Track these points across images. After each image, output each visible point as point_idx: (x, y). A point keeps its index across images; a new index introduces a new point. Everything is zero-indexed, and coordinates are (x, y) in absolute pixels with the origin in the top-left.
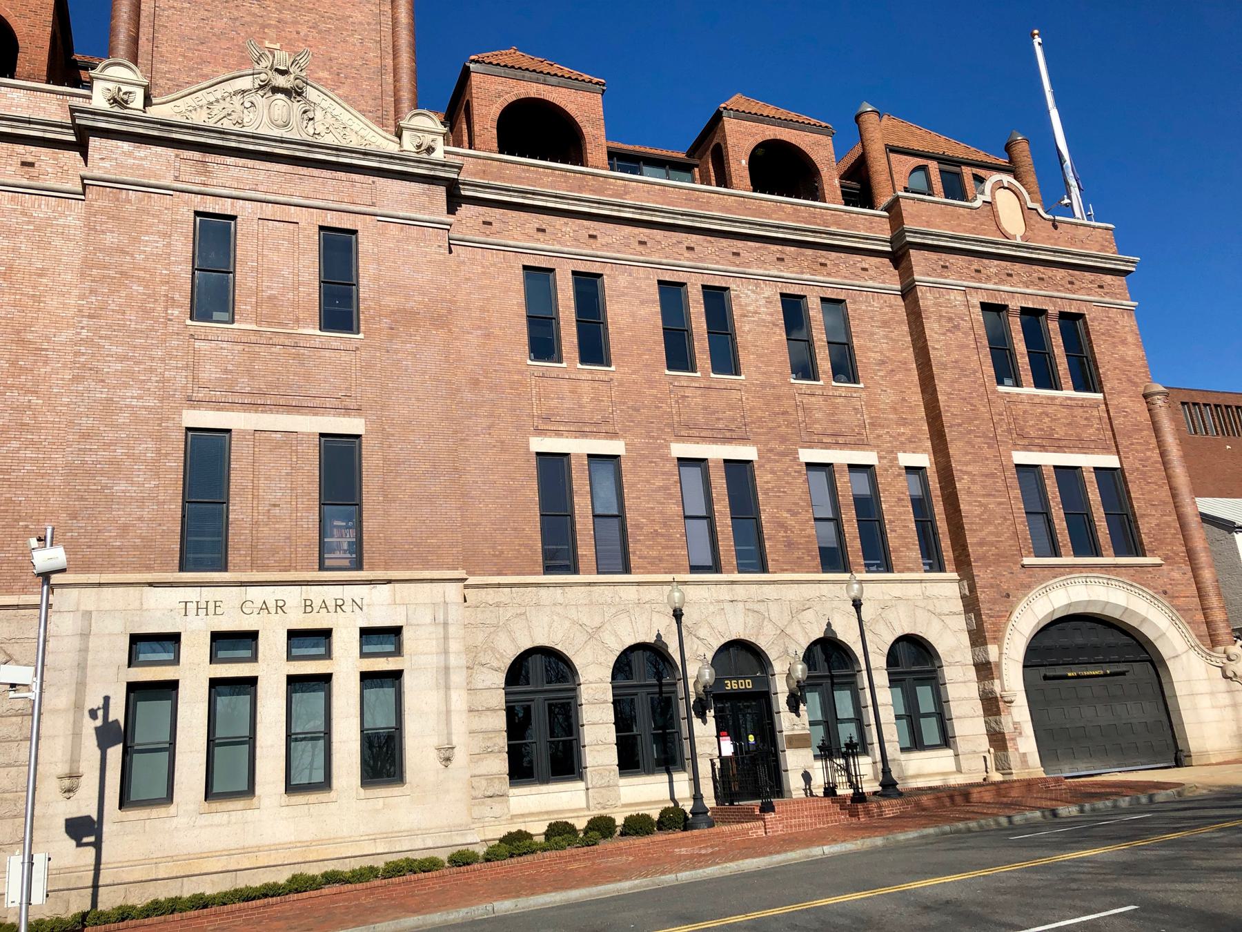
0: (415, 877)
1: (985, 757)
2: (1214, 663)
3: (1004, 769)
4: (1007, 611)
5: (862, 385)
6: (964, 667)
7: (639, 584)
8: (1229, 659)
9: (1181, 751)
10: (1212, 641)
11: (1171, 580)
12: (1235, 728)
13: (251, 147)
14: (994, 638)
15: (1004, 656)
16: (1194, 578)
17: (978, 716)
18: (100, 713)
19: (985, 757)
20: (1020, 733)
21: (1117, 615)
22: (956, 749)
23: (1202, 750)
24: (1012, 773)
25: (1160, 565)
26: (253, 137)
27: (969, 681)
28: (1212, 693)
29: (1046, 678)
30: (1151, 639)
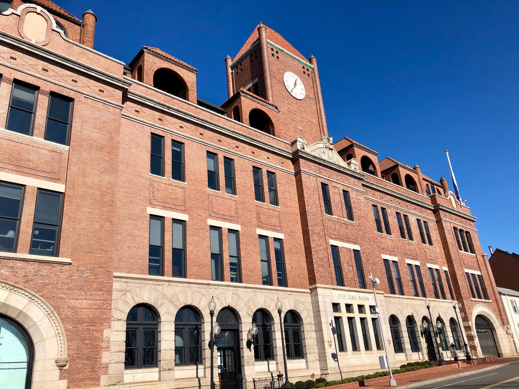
0: (409, 372)
5: (434, 247)
7: (407, 298)
8: (508, 329)
10: (503, 324)
13: (329, 165)
18: (331, 324)
25: (492, 303)
26: (330, 163)
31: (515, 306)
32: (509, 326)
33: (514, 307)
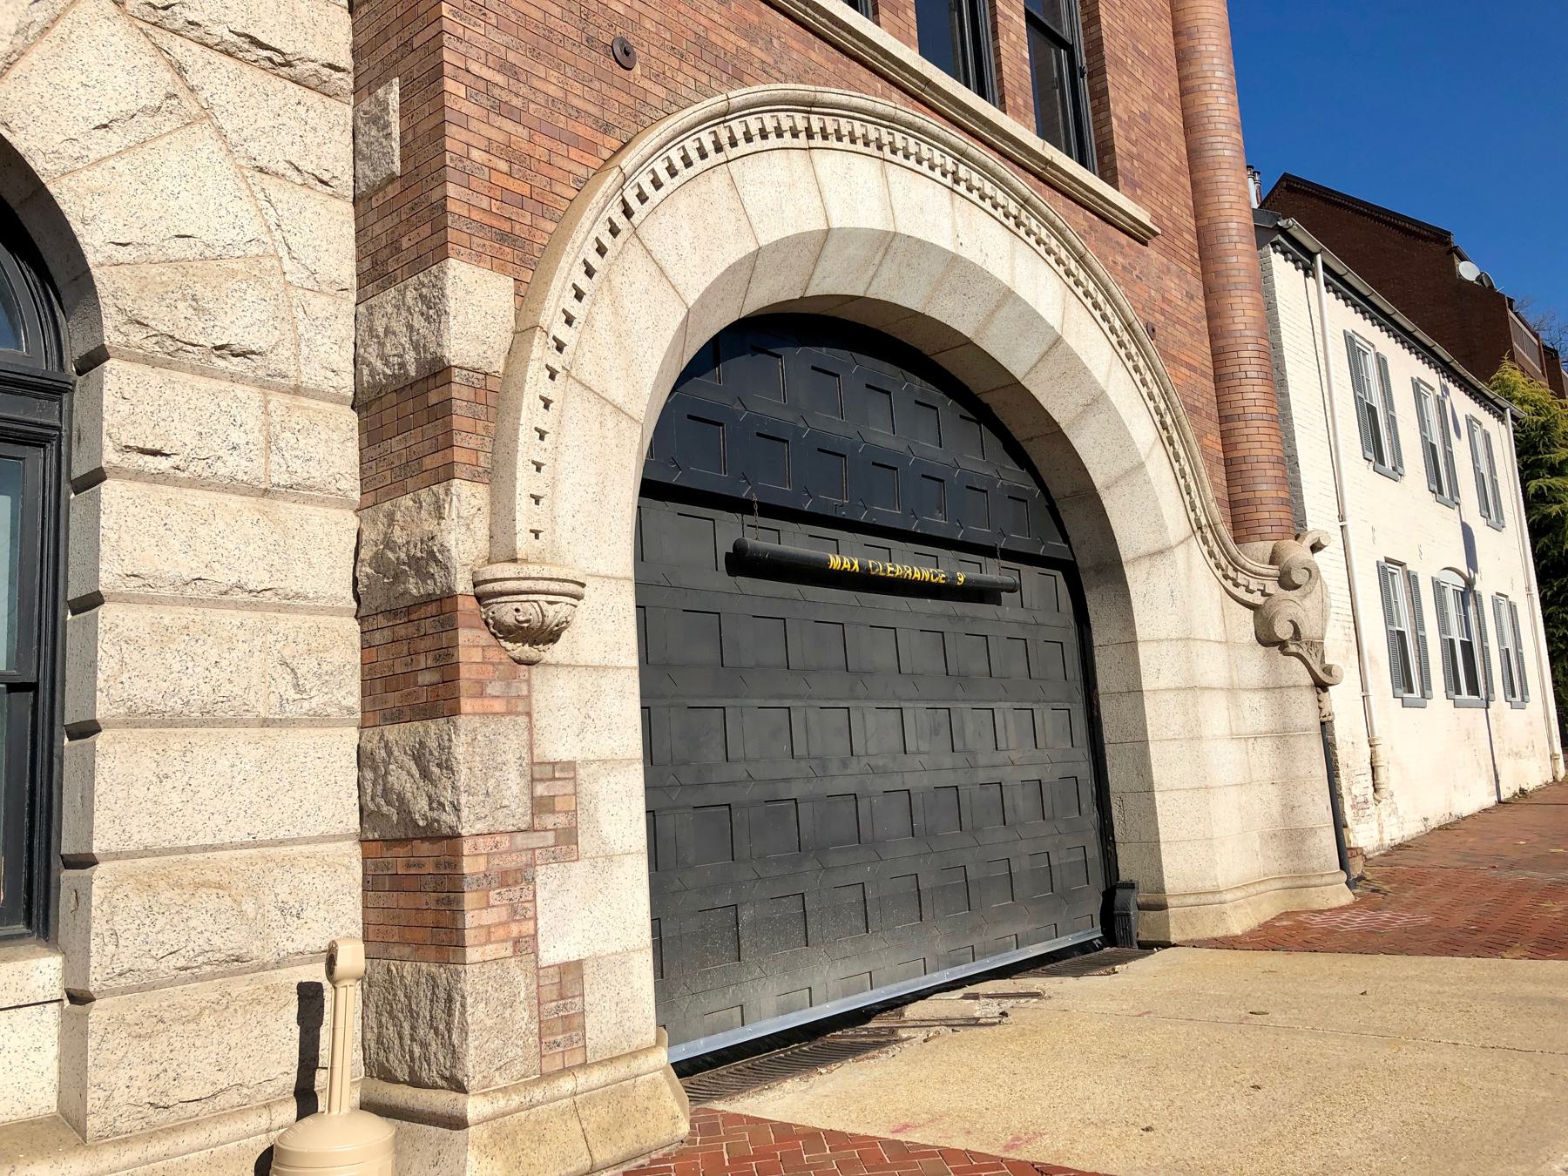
1: (310, 999)
2: (1240, 592)
3: (416, 1082)
4: (606, 129)
6: (278, 401)
8: (1286, 582)
9: (1131, 886)
11: (1164, 299)
12: (1275, 809)
14: (504, 237)
15: (540, 352)
16: (1209, 318)
17: (318, 720)
19: (310, 999)
20: (568, 836)
21: (1018, 360)
22: (77, 961)
24: (457, 1123)
27: (296, 491)
28: (1232, 690)
29: (742, 562)
30: (1098, 479)
31: (1378, 402)
32: (1297, 552)
33: (1372, 410)
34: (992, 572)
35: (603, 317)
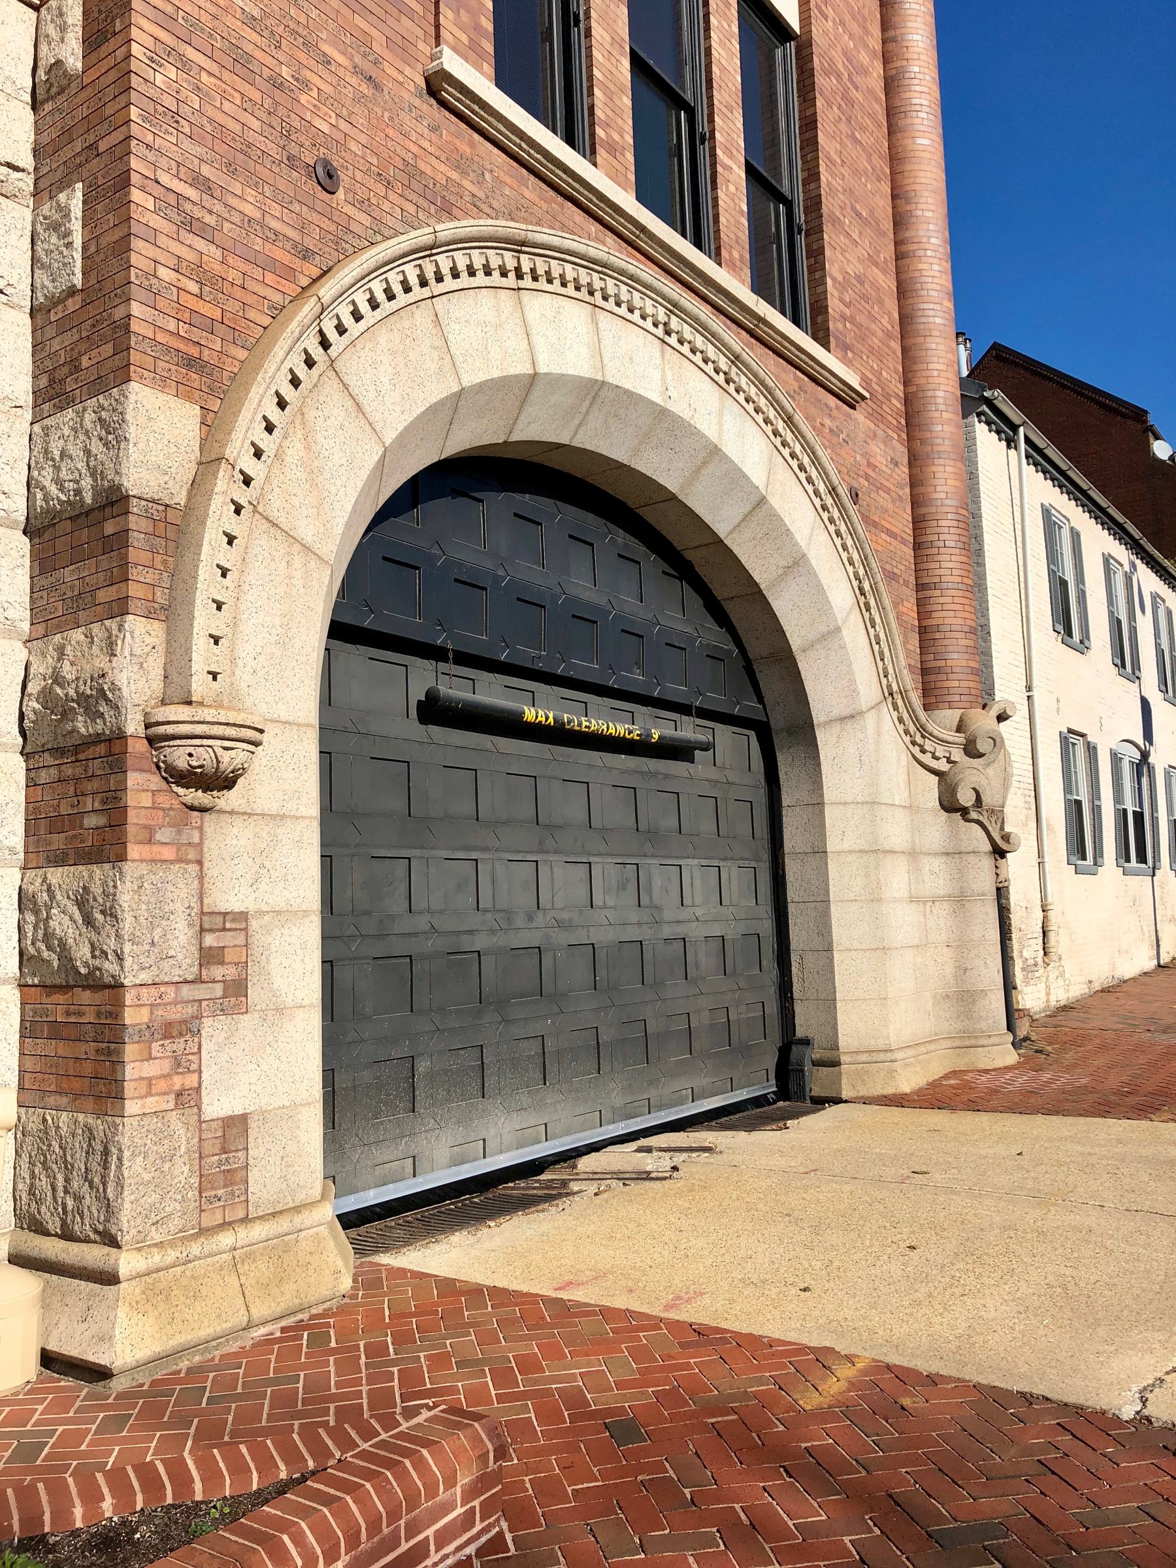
2: (927, 759)
3: (67, 1235)
4: (306, 254)
8: (971, 750)
9: (806, 1042)
11: (869, 464)
12: (949, 970)
14: (191, 363)
15: (225, 486)
16: (913, 485)
20: (237, 989)
23: (872, 1044)
24: (109, 1278)
28: (913, 854)
30: (795, 642)
31: (1070, 577)
32: (983, 721)
33: (1064, 583)
34: (688, 730)
35: (295, 451)
